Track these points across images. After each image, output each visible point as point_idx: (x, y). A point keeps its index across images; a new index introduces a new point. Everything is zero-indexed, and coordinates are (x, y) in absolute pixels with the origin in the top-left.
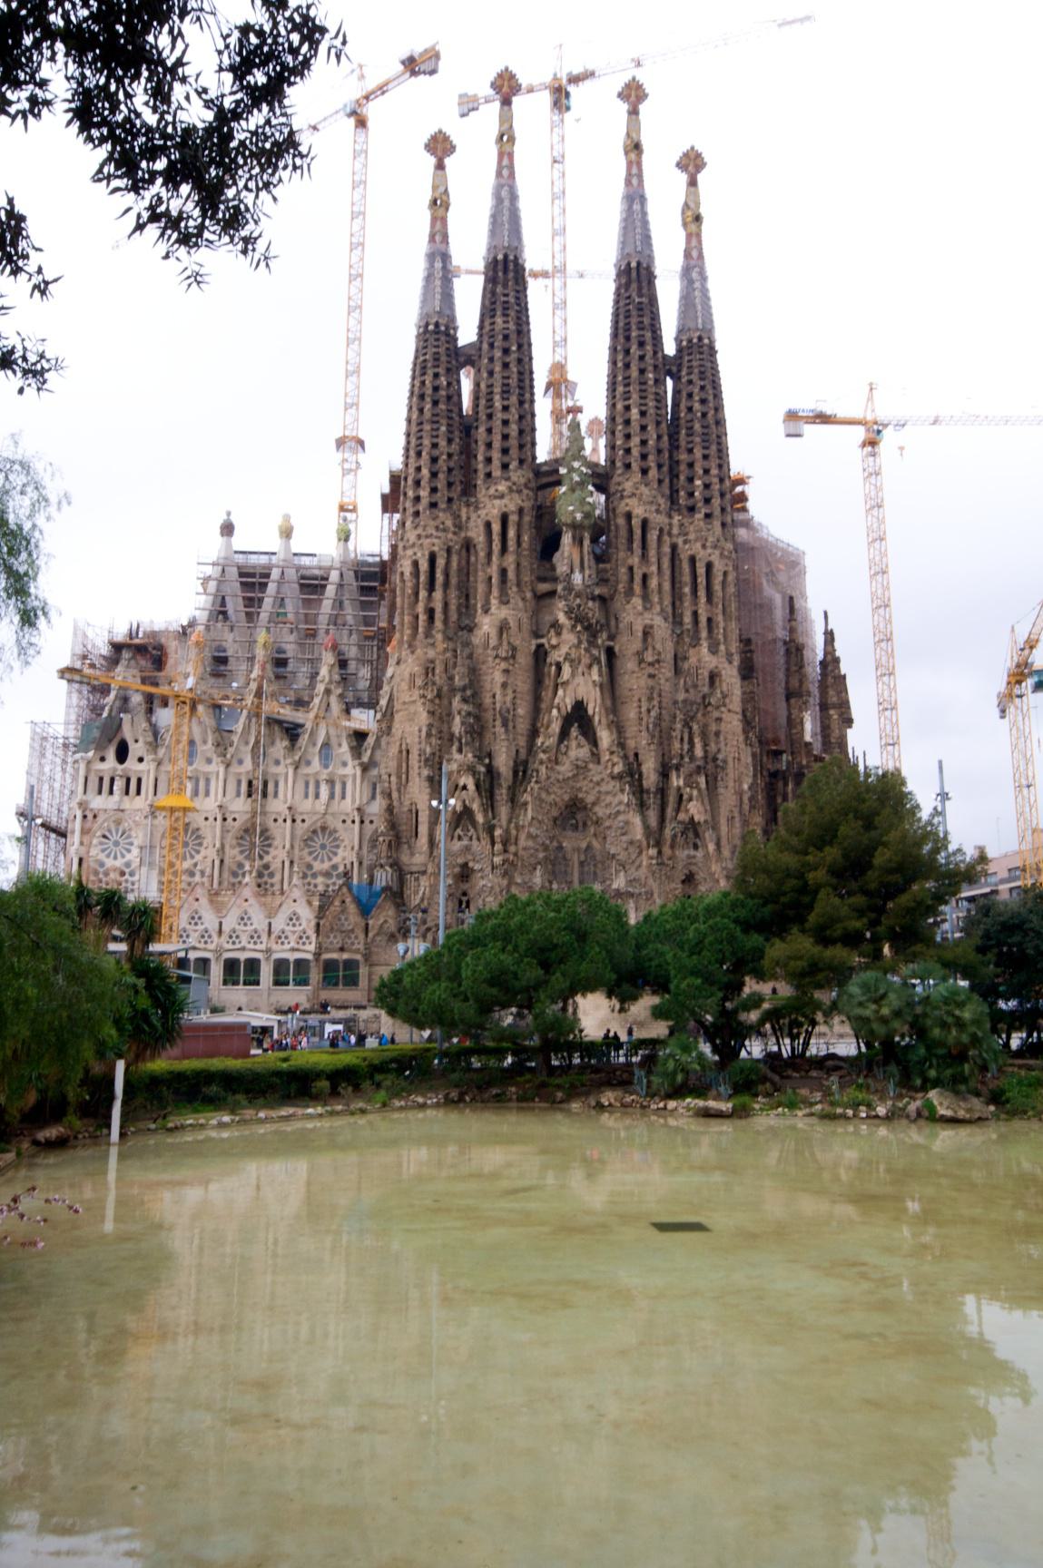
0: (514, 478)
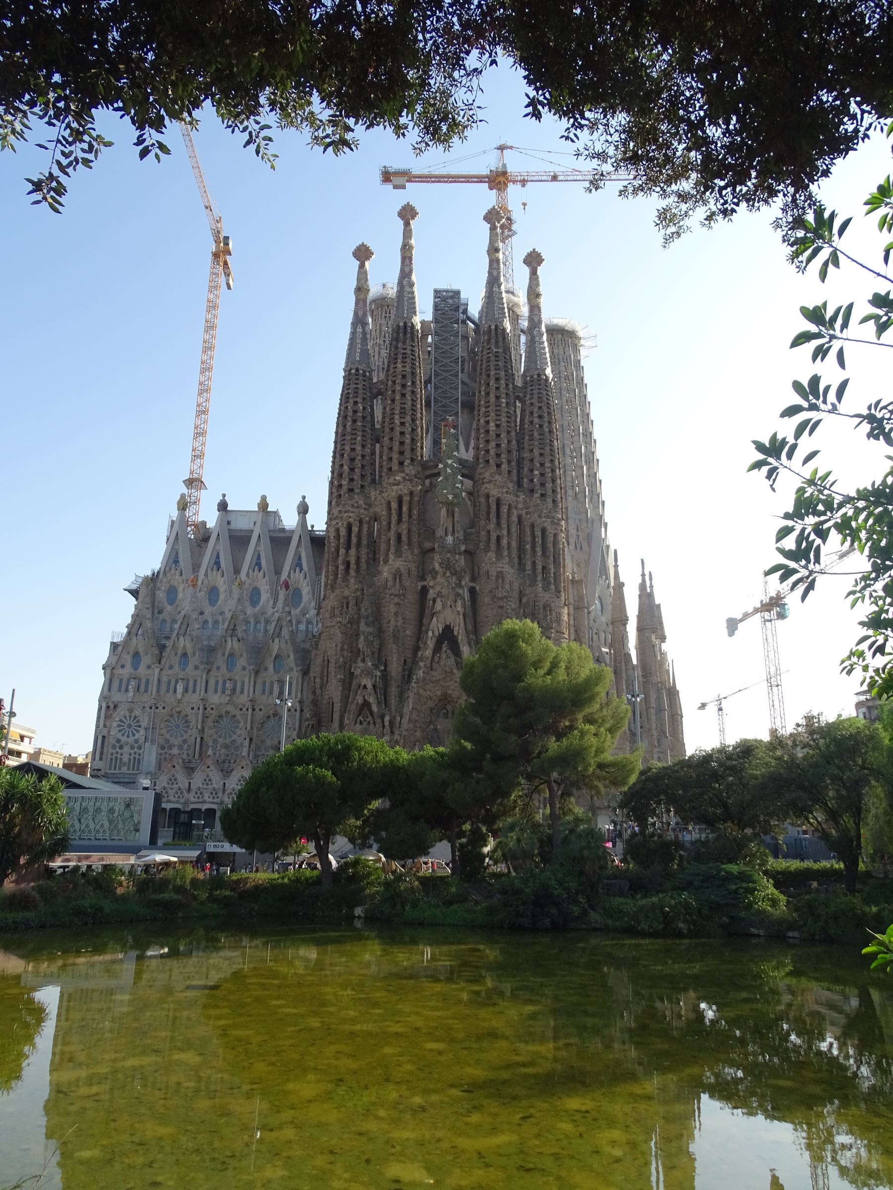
0: (407, 471)
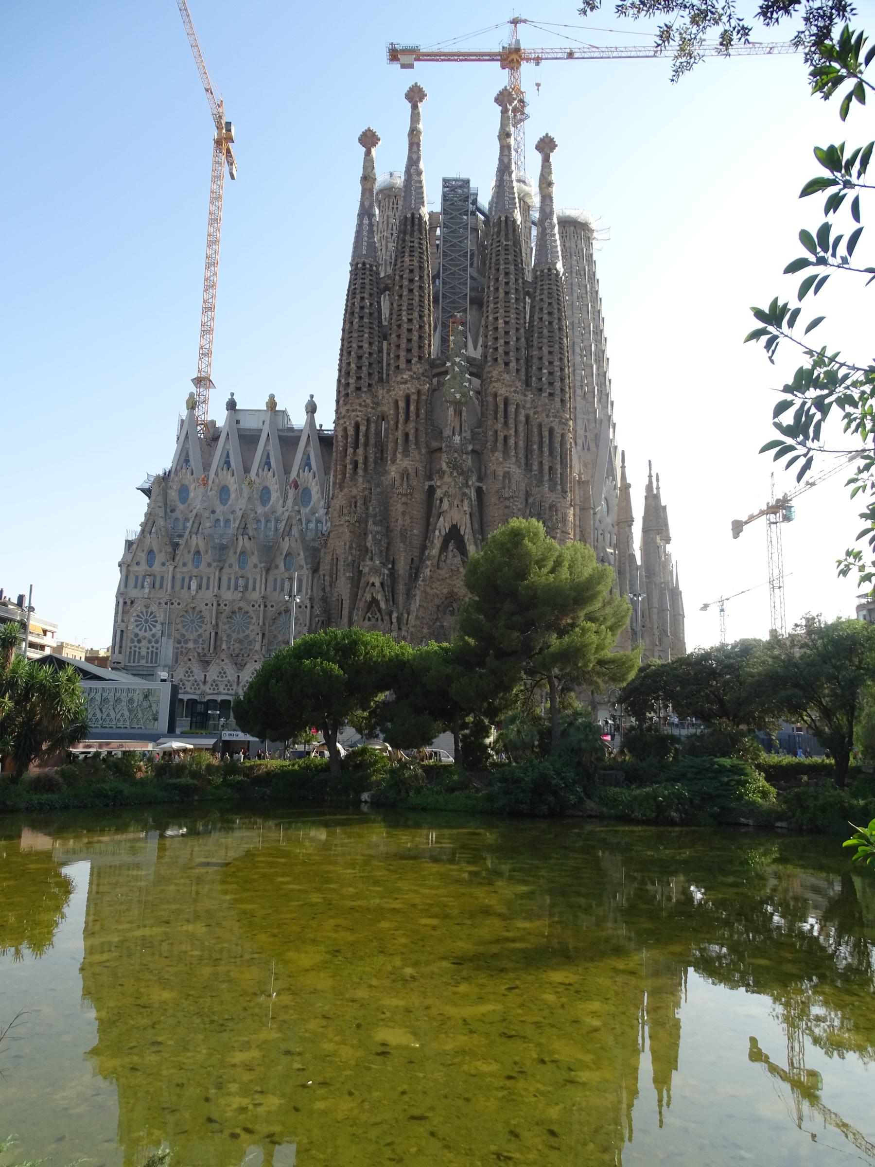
0: (415, 370)
